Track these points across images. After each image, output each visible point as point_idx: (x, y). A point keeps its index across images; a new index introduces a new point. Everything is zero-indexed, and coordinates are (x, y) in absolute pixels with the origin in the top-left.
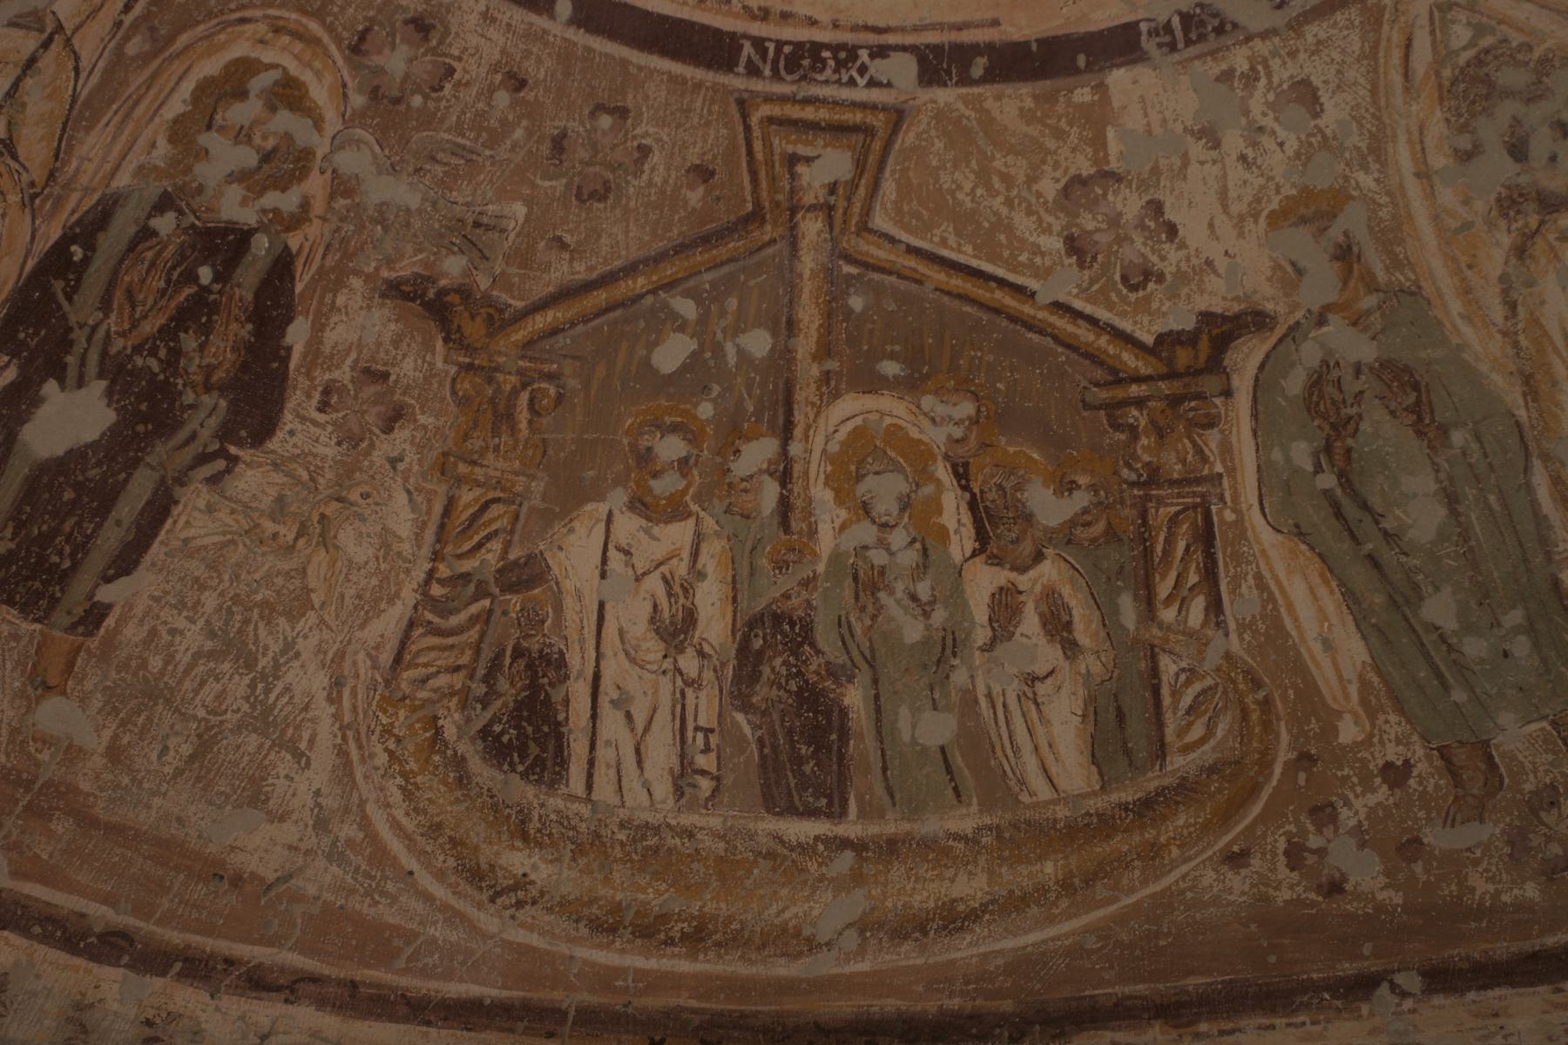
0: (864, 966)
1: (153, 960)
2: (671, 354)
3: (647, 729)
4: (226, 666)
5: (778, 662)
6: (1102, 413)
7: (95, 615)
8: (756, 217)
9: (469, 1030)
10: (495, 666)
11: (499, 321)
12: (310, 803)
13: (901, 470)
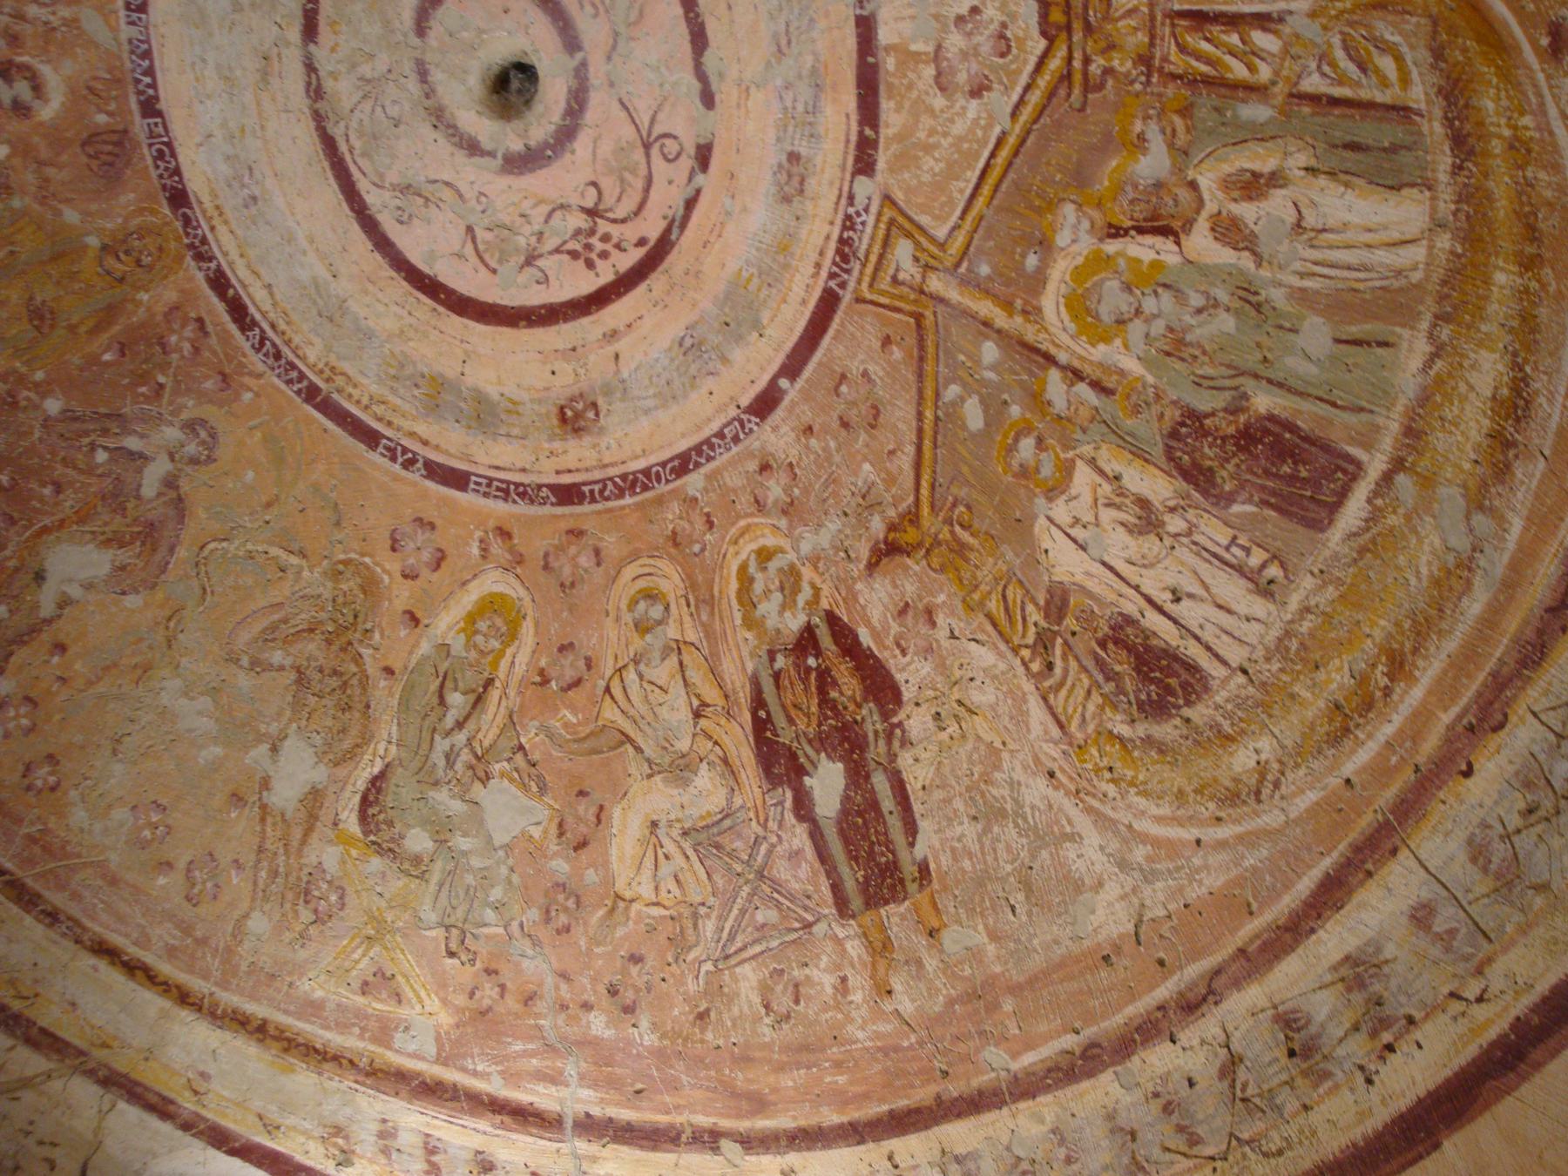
0: (1517, 525)
1: (1125, 1046)
2: (974, 415)
3: (1207, 588)
4: (996, 829)
5: (1206, 450)
6: (1090, 96)
7: (924, 870)
8: (918, 318)
9: (1342, 907)
10: (1101, 664)
11: (913, 517)
12: (1105, 859)
13: (1103, 280)
